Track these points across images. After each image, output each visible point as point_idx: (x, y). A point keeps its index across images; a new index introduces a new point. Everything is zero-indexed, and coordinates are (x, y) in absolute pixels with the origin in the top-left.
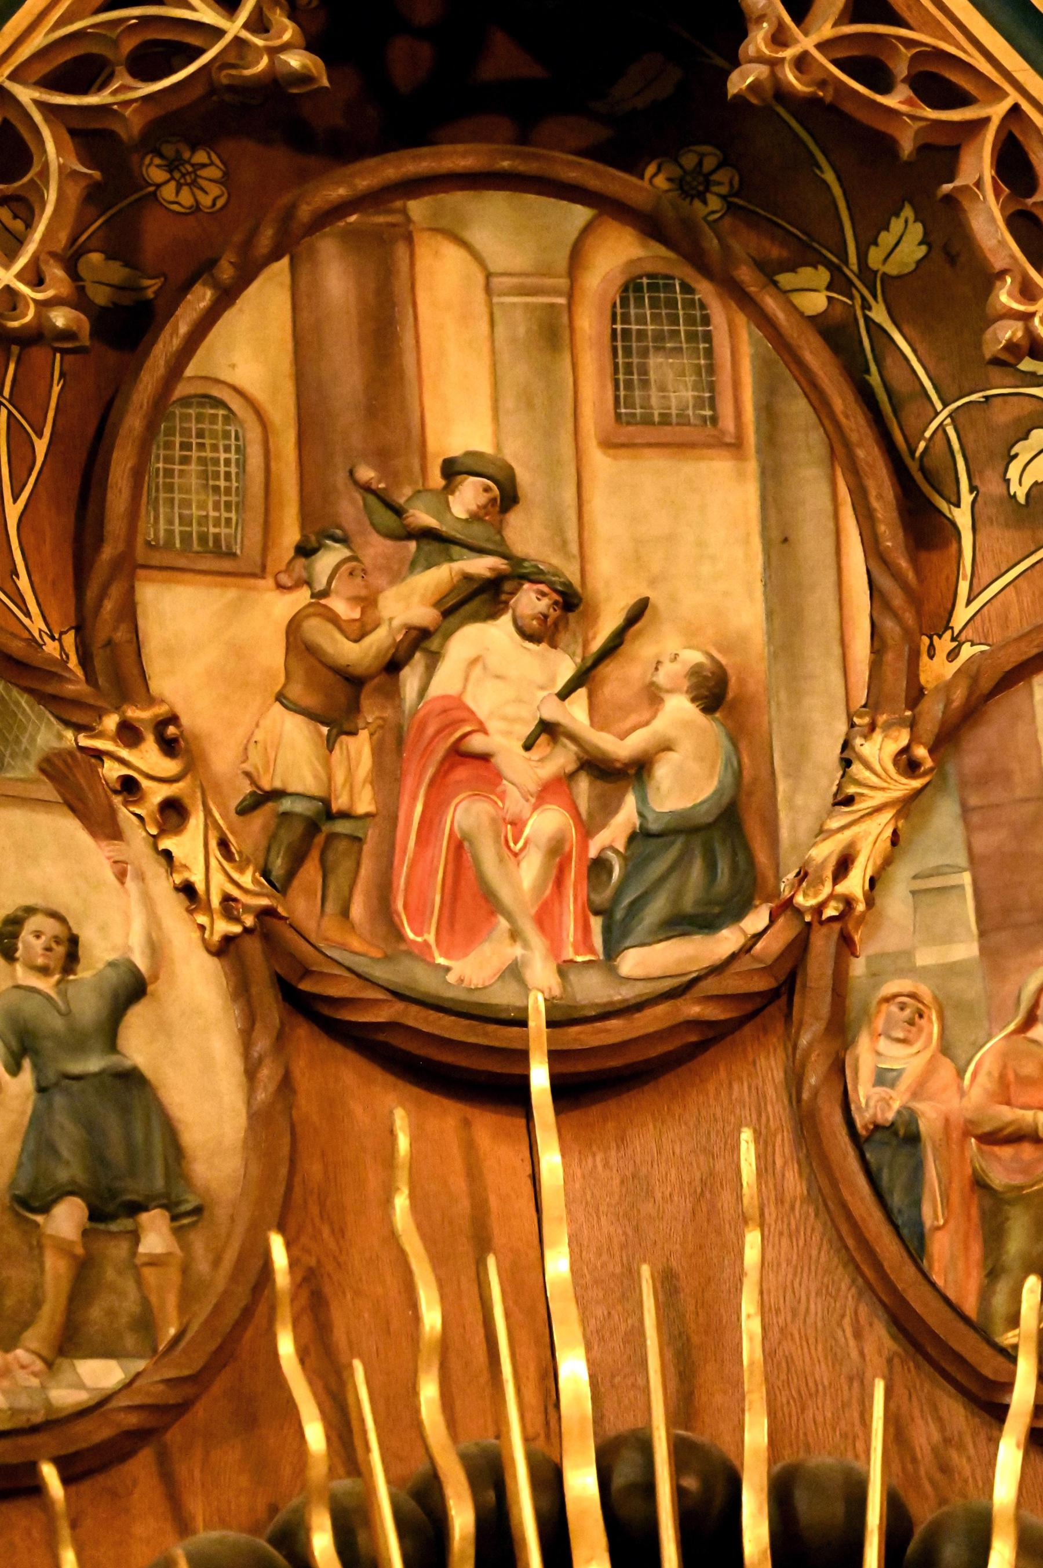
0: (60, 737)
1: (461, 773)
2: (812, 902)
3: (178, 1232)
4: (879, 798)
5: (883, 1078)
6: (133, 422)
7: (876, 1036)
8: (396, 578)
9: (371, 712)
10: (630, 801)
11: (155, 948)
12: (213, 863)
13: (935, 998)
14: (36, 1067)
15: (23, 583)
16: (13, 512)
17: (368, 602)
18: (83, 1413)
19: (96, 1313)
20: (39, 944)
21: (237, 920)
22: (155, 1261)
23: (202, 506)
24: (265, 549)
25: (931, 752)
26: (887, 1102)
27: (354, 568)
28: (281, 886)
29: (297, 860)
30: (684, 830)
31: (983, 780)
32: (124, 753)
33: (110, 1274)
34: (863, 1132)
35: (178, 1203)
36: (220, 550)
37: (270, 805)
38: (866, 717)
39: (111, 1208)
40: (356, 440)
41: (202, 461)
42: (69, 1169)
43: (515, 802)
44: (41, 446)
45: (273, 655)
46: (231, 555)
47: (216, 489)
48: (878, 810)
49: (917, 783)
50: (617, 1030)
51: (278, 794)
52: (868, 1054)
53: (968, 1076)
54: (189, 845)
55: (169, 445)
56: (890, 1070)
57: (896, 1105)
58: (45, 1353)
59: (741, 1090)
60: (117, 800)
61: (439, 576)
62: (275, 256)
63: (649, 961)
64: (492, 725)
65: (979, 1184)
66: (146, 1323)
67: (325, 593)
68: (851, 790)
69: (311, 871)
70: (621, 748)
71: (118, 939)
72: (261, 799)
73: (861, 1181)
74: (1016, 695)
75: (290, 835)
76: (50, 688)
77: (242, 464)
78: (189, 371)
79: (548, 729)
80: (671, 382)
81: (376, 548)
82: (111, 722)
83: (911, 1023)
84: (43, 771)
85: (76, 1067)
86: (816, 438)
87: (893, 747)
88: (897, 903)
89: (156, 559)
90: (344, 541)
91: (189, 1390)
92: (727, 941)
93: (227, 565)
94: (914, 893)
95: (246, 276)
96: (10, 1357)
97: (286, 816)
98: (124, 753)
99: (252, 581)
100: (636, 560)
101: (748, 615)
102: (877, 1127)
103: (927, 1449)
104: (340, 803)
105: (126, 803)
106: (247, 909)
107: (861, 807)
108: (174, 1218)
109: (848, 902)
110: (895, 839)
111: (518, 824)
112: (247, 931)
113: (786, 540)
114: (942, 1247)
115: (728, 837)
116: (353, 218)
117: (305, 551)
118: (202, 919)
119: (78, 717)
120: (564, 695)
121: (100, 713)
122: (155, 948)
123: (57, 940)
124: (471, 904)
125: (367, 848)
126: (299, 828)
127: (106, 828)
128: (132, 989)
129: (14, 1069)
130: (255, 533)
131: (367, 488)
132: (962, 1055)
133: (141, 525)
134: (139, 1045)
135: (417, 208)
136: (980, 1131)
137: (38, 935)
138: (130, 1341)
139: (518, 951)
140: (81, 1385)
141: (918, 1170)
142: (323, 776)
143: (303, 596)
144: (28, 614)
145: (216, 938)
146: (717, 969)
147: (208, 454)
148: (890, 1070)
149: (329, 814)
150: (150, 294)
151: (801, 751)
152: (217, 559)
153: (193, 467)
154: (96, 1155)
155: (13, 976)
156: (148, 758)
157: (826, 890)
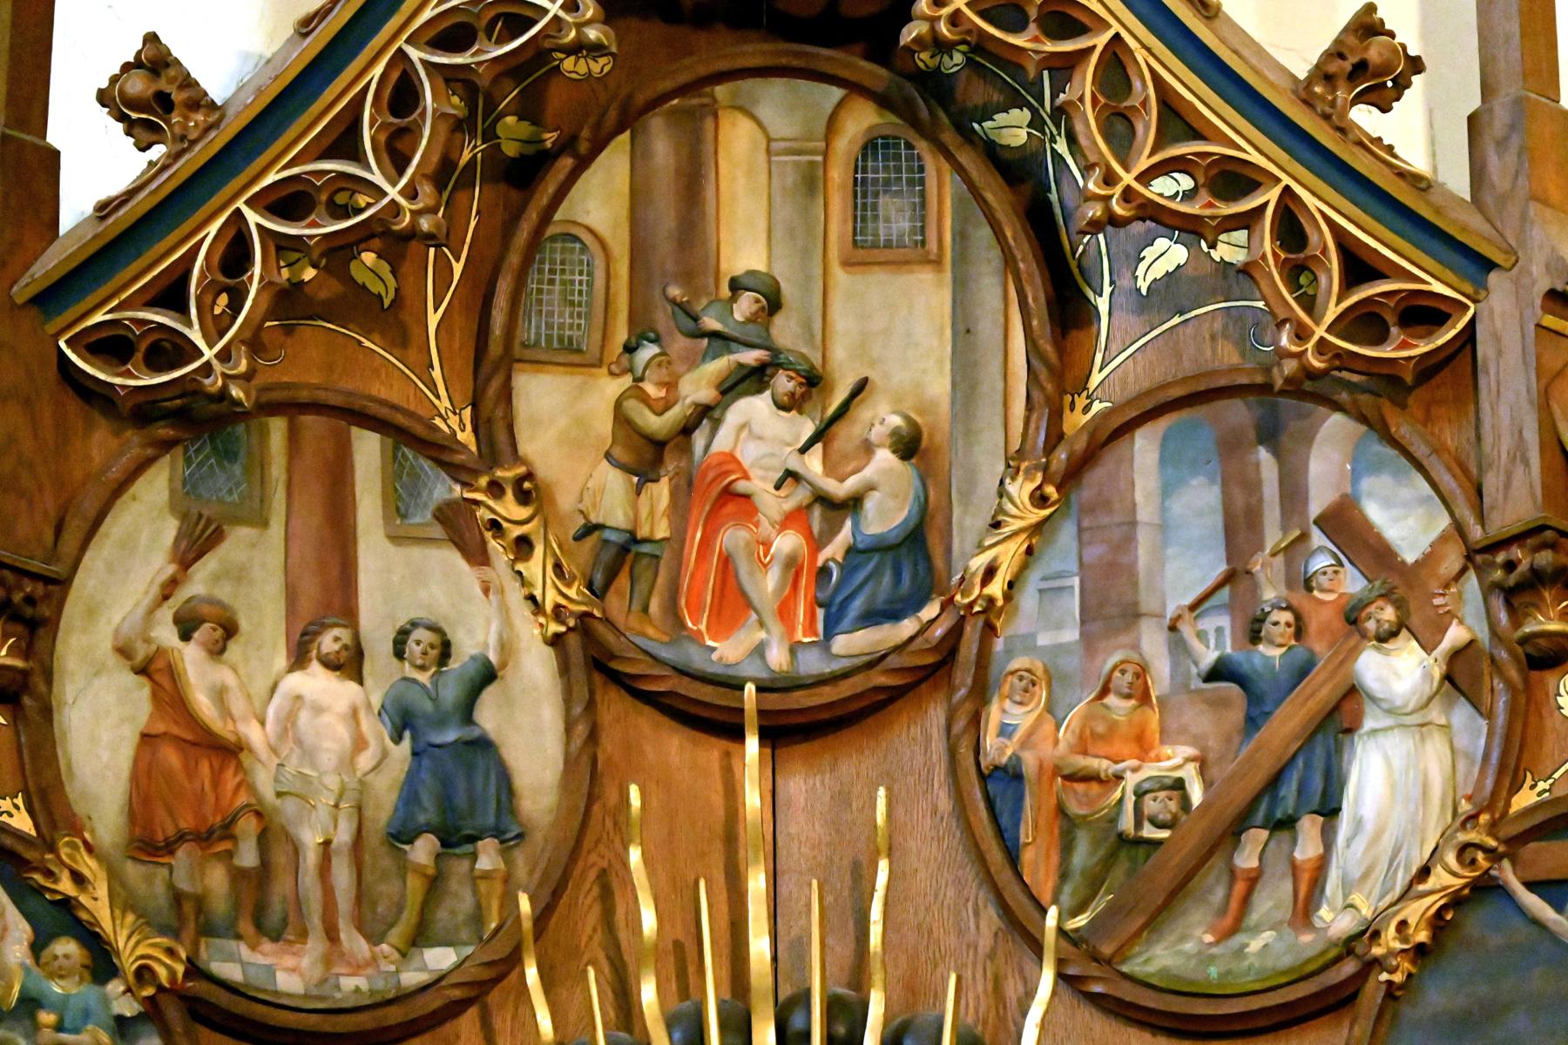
0: (451, 490)
1: (730, 508)
2: (967, 601)
3: (505, 853)
4: (1017, 525)
5: (1005, 731)
6: (514, 259)
7: (1002, 698)
8: (693, 362)
9: (671, 465)
10: (848, 523)
11: (505, 647)
12: (549, 581)
13: (1046, 671)
14: (414, 739)
15: (437, 373)
16: (433, 320)
17: (671, 385)
18: (424, 988)
19: (442, 915)
20: (418, 649)
21: (563, 623)
22: (486, 876)
23: (561, 315)
24: (603, 347)
25: (1058, 490)
26: (1001, 750)
27: (663, 359)
28: (598, 592)
29: (612, 575)
30: (881, 547)
31: (1090, 509)
32: (491, 503)
33: (453, 885)
34: (986, 772)
35: (504, 833)
36: (571, 347)
37: (596, 534)
38: (1013, 464)
39: (454, 839)
40: (670, 266)
41: (563, 282)
42: (428, 813)
43: (766, 528)
44: (458, 268)
45: (604, 425)
46: (579, 351)
47: (572, 303)
48: (1015, 534)
49: (1047, 512)
50: (828, 694)
51: (599, 527)
52: (994, 715)
53: (1062, 730)
54: (534, 568)
55: (541, 271)
56: (1013, 725)
57: (1009, 752)
58: (401, 946)
59: (916, 731)
60: (488, 535)
61: (718, 366)
62: (620, 131)
63: (853, 643)
64: (752, 474)
65: (1061, 810)
66: (478, 918)
67: (641, 379)
68: (1000, 518)
69: (623, 580)
70: (839, 489)
71: (480, 637)
72: (590, 529)
73: (982, 805)
74: (1120, 446)
75: (607, 556)
76: (446, 457)
77: (590, 284)
78: (558, 216)
79: (791, 476)
80: (894, 217)
81: (680, 344)
82: (483, 481)
83: (1026, 691)
84: (435, 517)
85: (438, 740)
86: (995, 254)
87: (1030, 486)
88: (1028, 599)
89: (528, 354)
90: (656, 340)
91: (502, 968)
92: (908, 627)
93: (576, 358)
94: (1040, 591)
95: (598, 147)
96: (377, 949)
97: (606, 542)
98: (491, 503)
99: (593, 370)
100: (862, 349)
101: (939, 386)
102: (996, 768)
103: (1014, 998)
104: (643, 533)
105: (494, 537)
106: (572, 613)
107: (1006, 530)
108: (502, 842)
109: (991, 600)
110: (1029, 551)
111: (767, 545)
112: (569, 629)
113: (968, 331)
114: (1028, 856)
115: (915, 553)
116: (675, 101)
117: (630, 349)
118: (542, 620)
119: (465, 477)
120: (803, 450)
121: (476, 473)
122: (505, 647)
123: (432, 646)
124: (732, 603)
125: (662, 562)
126: (613, 551)
127: (478, 556)
128: (487, 675)
129: (397, 739)
130: (597, 336)
131: (673, 302)
132: (1060, 715)
133: (518, 332)
134: (488, 716)
135: (721, 91)
136: (1066, 772)
137: (418, 643)
138: (464, 934)
139: (762, 635)
140: (424, 968)
141: (1020, 799)
142: (631, 514)
143: (627, 381)
144: (438, 397)
145: (550, 633)
146: (899, 648)
147: (567, 277)
148: (1013, 725)
149: (634, 540)
150: (549, 144)
151: (971, 482)
152: (572, 356)
153: (557, 287)
154: (446, 801)
155: (403, 670)
156: (509, 508)
157: (976, 592)
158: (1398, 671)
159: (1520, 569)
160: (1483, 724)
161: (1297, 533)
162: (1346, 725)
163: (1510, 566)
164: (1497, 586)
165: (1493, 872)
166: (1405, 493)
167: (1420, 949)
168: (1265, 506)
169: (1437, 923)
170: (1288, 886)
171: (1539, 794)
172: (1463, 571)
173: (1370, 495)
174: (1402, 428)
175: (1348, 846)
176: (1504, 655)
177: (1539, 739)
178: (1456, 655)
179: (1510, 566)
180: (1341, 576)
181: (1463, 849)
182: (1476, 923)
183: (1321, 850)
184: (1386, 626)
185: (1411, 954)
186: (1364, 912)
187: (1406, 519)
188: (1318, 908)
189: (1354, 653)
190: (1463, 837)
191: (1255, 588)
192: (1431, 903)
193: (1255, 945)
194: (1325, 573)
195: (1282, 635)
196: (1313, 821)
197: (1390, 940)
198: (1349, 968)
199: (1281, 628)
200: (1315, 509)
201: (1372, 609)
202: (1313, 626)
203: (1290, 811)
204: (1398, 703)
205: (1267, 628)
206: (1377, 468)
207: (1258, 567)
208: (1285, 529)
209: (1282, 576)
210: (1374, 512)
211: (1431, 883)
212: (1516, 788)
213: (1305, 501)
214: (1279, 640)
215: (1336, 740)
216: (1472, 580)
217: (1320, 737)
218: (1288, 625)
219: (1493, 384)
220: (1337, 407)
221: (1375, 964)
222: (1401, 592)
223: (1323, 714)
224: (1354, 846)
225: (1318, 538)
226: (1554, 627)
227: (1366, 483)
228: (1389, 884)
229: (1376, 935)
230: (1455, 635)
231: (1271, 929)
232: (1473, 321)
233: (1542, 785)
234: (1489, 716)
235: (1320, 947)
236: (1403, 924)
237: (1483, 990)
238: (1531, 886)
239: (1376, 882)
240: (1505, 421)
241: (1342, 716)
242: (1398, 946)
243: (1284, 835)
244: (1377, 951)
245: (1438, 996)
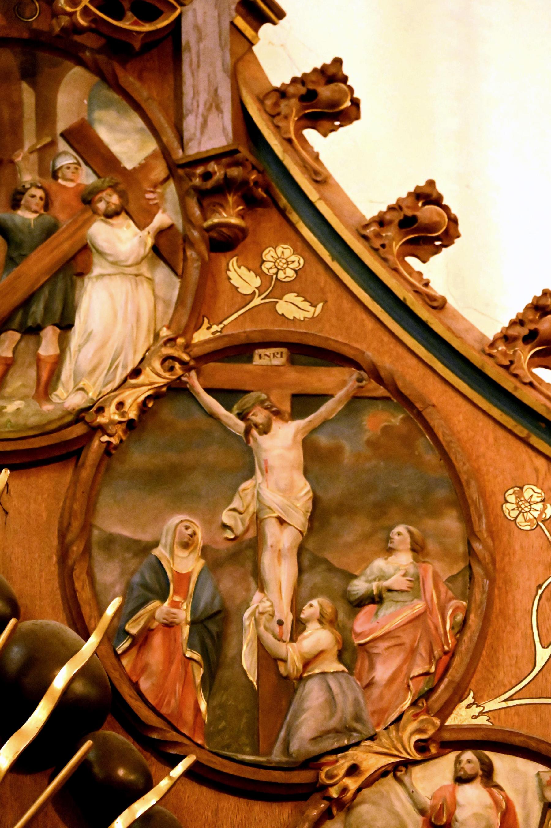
158: (121, 239)
159: (215, 178)
160: (177, 282)
161: (48, 140)
162: (79, 271)
163: (207, 176)
164: (196, 189)
165: (184, 379)
166: (126, 124)
167: (130, 425)
168: (25, 120)
169: (143, 407)
170: (33, 373)
171: (213, 333)
172: (166, 179)
173: (100, 121)
174: (128, 80)
175: (79, 351)
176: (196, 234)
177: (215, 295)
178: (161, 233)
179: (207, 176)
180: (80, 172)
181: (166, 359)
182: (167, 412)
183: (58, 351)
184: (113, 207)
185: (124, 426)
186: (90, 394)
187: (127, 141)
188: (55, 389)
189: (88, 223)
190: (168, 351)
191: (15, 173)
192: (143, 393)
193: (11, 408)
194: (69, 168)
195: (37, 204)
196: (54, 331)
197: (111, 414)
198: (79, 430)
199: (37, 200)
200: (61, 126)
201: (104, 194)
202: (57, 204)
203: (39, 321)
204: (122, 258)
205: (26, 198)
206: (107, 105)
207: (20, 159)
208: (39, 134)
209: (36, 167)
210: (103, 133)
211: (141, 379)
212: (198, 327)
213: (54, 122)
214: (34, 208)
215: (72, 280)
216: (171, 188)
217: (61, 276)
218: (41, 198)
219: (195, 59)
220: (81, 62)
221: (102, 429)
222: (121, 187)
223: (66, 260)
224: (84, 350)
225: (62, 145)
226: (234, 221)
227: (98, 114)
228: (110, 377)
229: (101, 410)
230: (161, 219)
231: (21, 399)
232: (179, 18)
233: (215, 328)
234: (181, 276)
235: (59, 413)
236: (121, 405)
237: (173, 457)
238: (209, 391)
239: (100, 376)
240: (203, 85)
241: (77, 264)
242: (117, 418)
243: (31, 339)
244: (101, 420)
245: (139, 457)
